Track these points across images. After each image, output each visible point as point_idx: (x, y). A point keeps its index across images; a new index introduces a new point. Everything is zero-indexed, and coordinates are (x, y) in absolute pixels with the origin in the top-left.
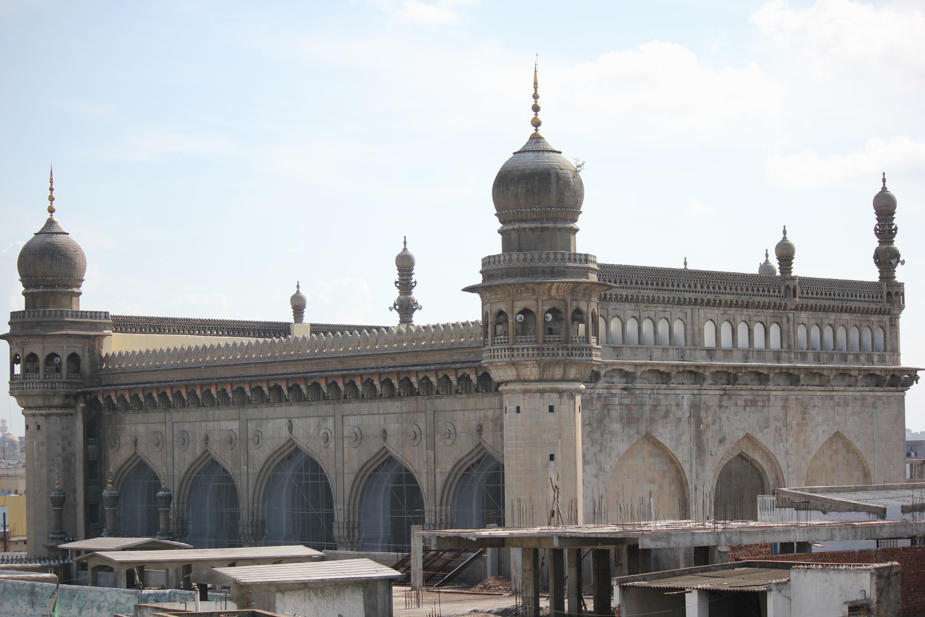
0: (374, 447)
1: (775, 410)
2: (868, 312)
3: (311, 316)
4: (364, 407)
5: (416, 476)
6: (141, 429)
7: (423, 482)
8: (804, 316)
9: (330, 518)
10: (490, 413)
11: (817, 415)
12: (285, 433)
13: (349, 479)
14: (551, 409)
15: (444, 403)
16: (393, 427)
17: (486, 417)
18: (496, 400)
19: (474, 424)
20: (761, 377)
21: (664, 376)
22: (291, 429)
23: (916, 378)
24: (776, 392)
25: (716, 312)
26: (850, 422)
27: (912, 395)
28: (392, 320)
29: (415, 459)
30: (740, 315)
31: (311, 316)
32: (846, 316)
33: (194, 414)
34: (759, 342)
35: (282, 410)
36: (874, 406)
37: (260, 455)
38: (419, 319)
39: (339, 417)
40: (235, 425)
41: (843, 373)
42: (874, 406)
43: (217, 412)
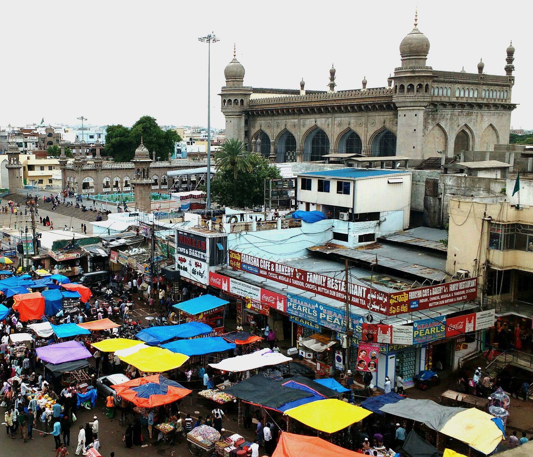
0: (345, 127)
1: (474, 117)
2: (504, 86)
3: (306, 88)
4: (343, 115)
5: (360, 136)
6: (263, 121)
7: (362, 138)
8: (485, 87)
9: (328, 148)
10: (388, 117)
11: (486, 118)
12: (314, 123)
13: (336, 137)
14: (416, 115)
15: (370, 114)
16: (353, 121)
17: (387, 118)
18: (391, 113)
19: (382, 120)
20: (471, 105)
21: (444, 105)
22: (316, 122)
23: (516, 107)
24: (475, 111)
25: (460, 86)
26: (494, 120)
27: (514, 112)
28: (328, 89)
29: (361, 132)
30: (466, 87)
31: (306, 88)
32: (497, 87)
33: (282, 117)
34: (471, 96)
35: (312, 116)
36: (502, 116)
37: (304, 130)
38: (336, 89)
39: (333, 118)
40: (296, 121)
41: (495, 105)
42: (502, 116)
43: (290, 117)
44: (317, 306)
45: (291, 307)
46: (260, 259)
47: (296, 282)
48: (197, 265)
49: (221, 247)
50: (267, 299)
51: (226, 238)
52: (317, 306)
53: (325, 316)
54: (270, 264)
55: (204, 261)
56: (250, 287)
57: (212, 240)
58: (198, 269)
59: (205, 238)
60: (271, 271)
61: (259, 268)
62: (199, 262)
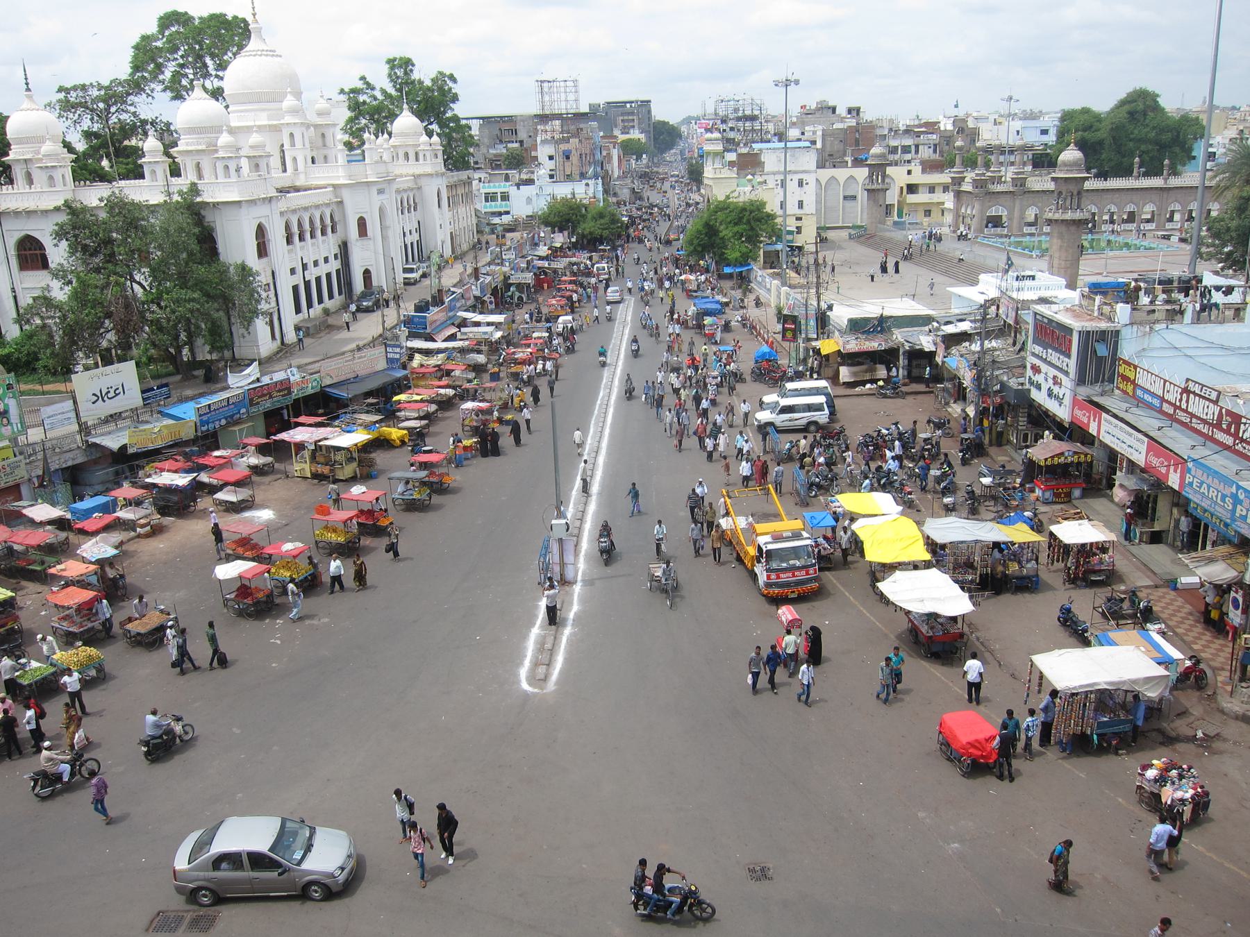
44: (1234, 490)
45: (1191, 484)
46: (1165, 381)
47: (1220, 436)
48: (1056, 381)
49: (1102, 350)
50: (1155, 462)
51: (1118, 332)
52: (1234, 490)
53: (1244, 513)
54: (1181, 394)
55: (1066, 373)
56: (1130, 435)
57: (1086, 336)
58: (1056, 389)
59: (1069, 330)
60: (1180, 408)
61: (1163, 400)
62: (1060, 375)
